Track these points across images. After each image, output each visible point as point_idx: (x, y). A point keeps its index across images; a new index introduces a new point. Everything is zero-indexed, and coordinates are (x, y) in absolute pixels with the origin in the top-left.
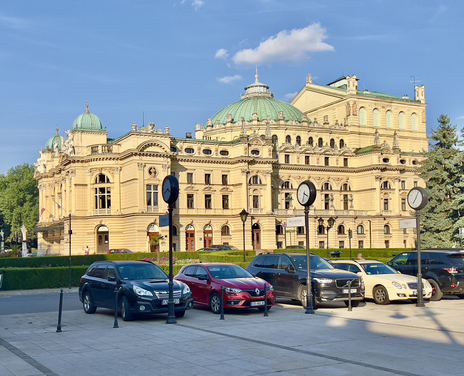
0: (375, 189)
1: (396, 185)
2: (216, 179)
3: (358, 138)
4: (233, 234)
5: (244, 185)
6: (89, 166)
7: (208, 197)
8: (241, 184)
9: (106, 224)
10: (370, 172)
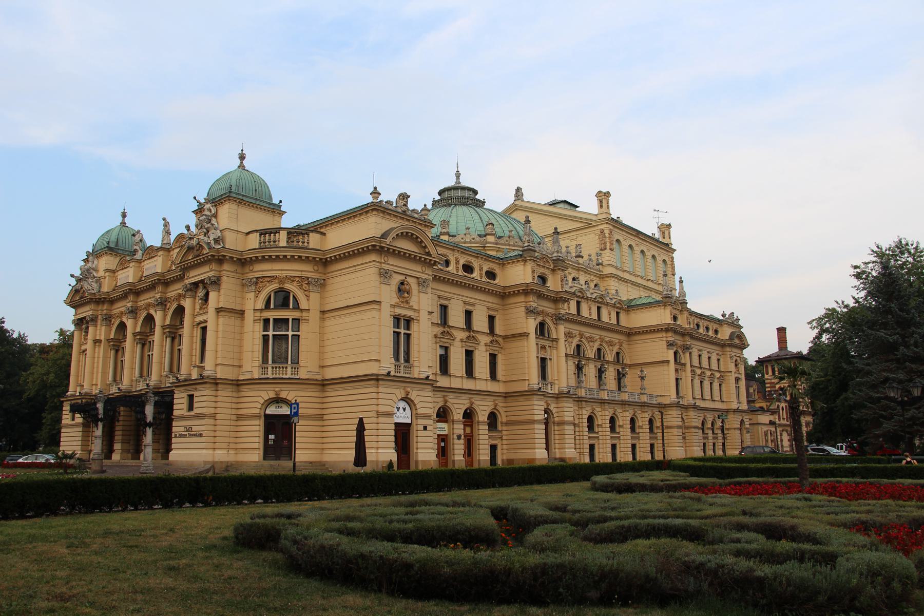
0: (668, 362)
1: (685, 358)
3: (617, 285)
4: (504, 428)
5: (533, 336)
7: (469, 354)
10: (660, 335)
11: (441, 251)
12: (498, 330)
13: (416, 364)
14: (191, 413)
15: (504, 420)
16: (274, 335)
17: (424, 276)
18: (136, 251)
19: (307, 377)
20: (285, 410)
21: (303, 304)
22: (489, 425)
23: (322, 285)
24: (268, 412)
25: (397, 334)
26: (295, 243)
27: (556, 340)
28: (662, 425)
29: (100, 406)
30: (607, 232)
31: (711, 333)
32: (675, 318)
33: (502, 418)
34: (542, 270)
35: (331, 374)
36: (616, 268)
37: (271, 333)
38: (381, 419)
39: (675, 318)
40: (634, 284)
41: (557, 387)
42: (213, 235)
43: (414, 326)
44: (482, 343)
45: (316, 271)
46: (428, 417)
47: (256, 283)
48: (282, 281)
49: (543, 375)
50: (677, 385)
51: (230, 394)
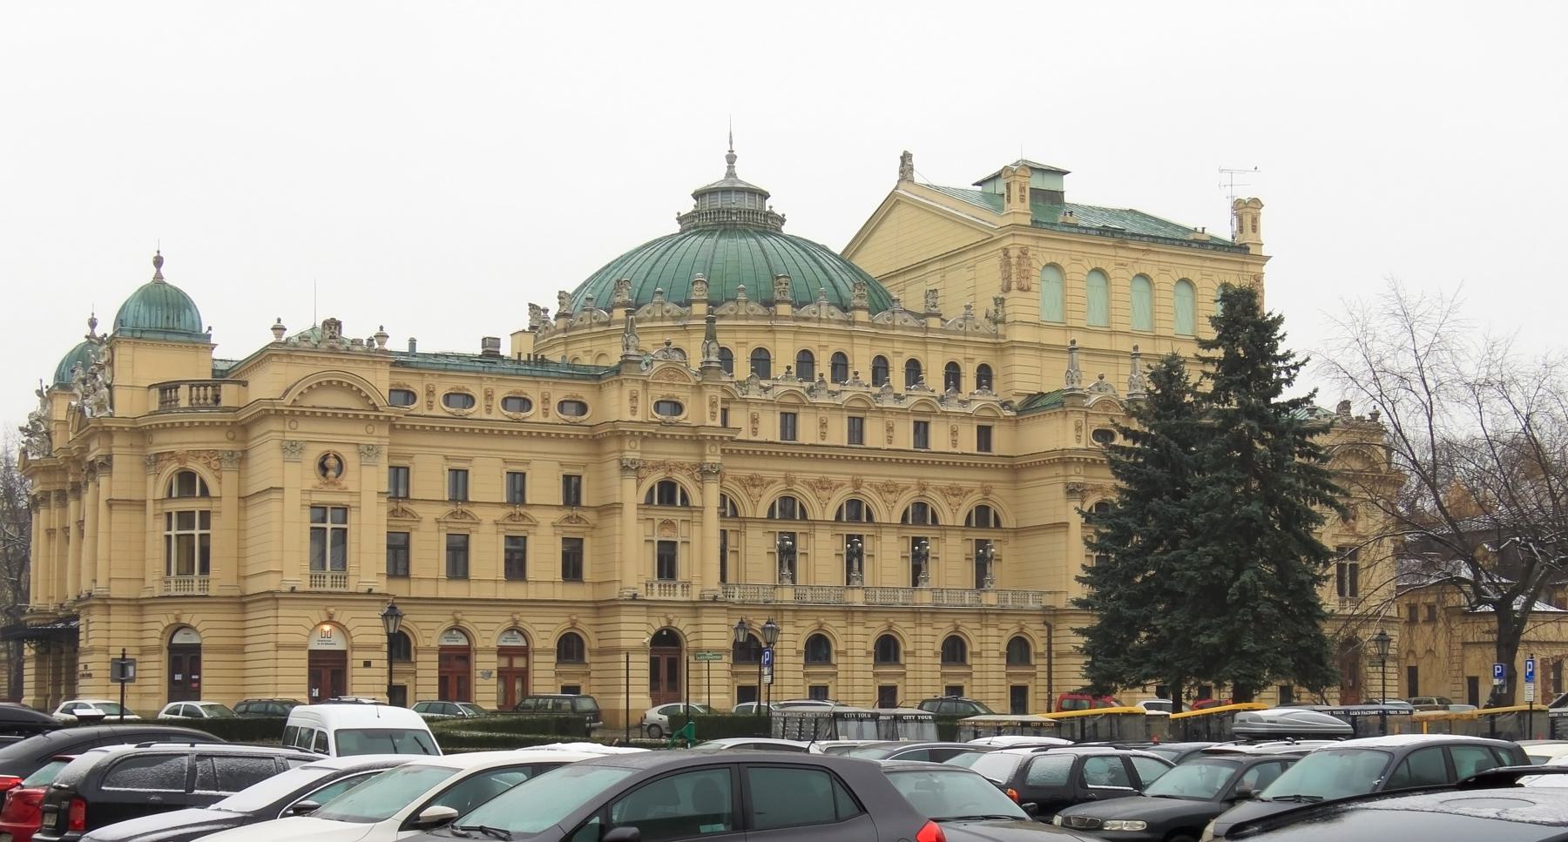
2: (544, 487)
4: (594, 659)
5: (631, 511)
9: (193, 624)
13: (351, 572)
17: (373, 441)
20: (192, 639)
21: (214, 491)
23: (241, 459)
24: (175, 641)
27: (701, 510)
33: (591, 642)
35: (254, 586)
37: (174, 532)
38: (281, 653)
43: (352, 517)
47: (156, 462)
51: (126, 618)
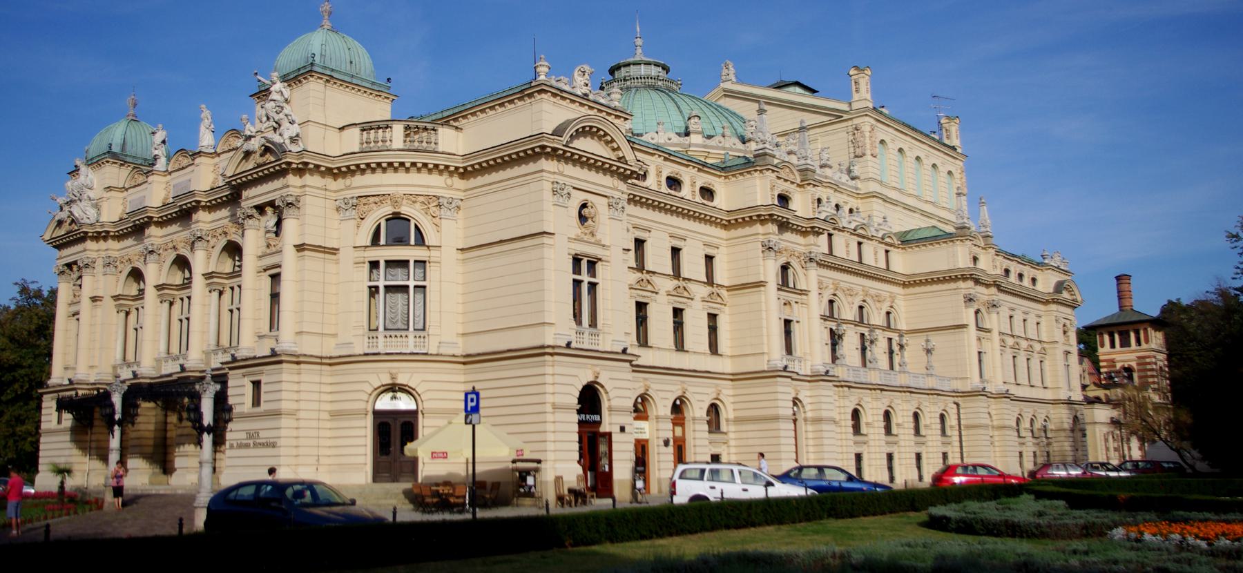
0: (964, 326)
4: (732, 428)
6: (348, 188)
7: (678, 312)
8: (760, 284)
10: (953, 285)
11: (640, 156)
12: (719, 278)
13: (606, 329)
14: (257, 410)
15: (731, 415)
16: (386, 287)
17: (617, 194)
18: (156, 158)
19: (442, 351)
20: (404, 403)
22: (709, 423)
25: (577, 283)
26: (416, 144)
28: (959, 425)
29: (117, 400)
30: (866, 129)
31: (1026, 282)
32: (975, 259)
33: (727, 413)
34: (782, 187)
36: (881, 183)
37: (381, 284)
39: (975, 259)
40: (907, 207)
41: (809, 364)
42: (289, 131)
44: (698, 298)
45: (450, 187)
46: (621, 411)
48: (395, 202)
49: (789, 349)
50: (980, 361)
